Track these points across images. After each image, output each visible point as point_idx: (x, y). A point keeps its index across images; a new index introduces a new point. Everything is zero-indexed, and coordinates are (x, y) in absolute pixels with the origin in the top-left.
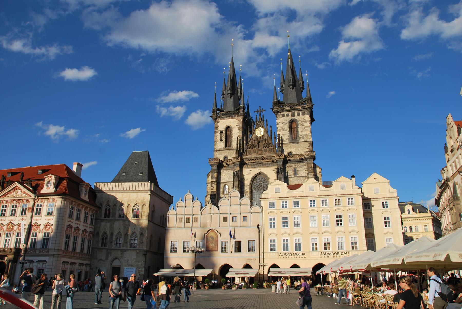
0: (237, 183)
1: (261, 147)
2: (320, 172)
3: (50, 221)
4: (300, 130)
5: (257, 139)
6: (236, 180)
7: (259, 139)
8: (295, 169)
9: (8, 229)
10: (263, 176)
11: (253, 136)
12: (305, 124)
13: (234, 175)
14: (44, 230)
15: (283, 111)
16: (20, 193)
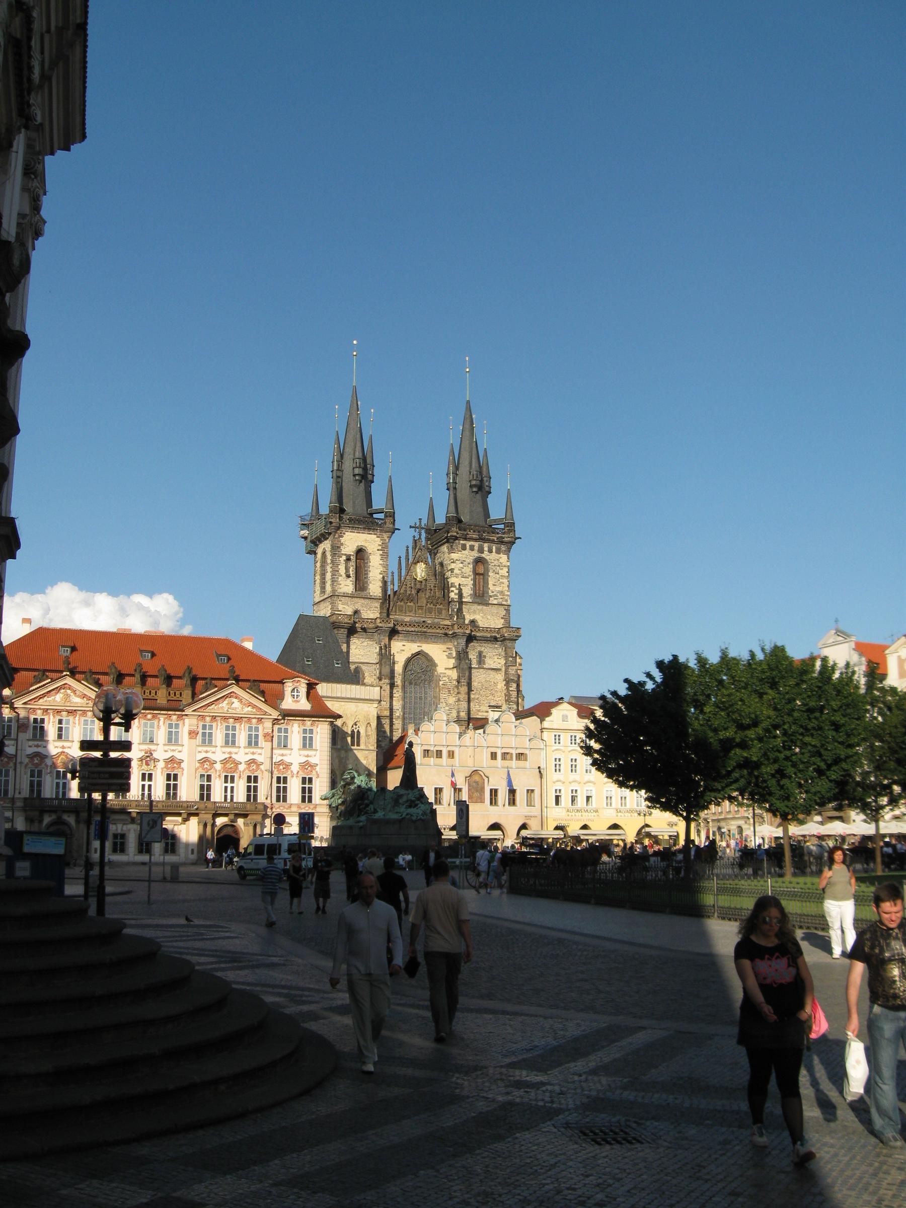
0: (386, 670)
1: (423, 602)
2: (520, 665)
3: (309, 759)
4: (491, 582)
5: (415, 584)
6: (385, 663)
7: (418, 586)
8: (480, 653)
9: (225, 769)
10: (423, 658)
11: (408, 578)
12: (500, 572)
13: (380, 654)
14: (301, 772)
15: (465, 539)
16: (236, 703)
